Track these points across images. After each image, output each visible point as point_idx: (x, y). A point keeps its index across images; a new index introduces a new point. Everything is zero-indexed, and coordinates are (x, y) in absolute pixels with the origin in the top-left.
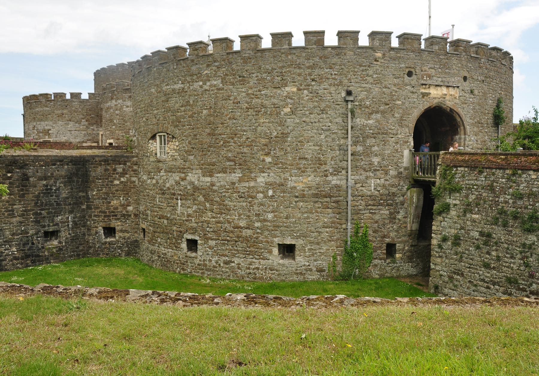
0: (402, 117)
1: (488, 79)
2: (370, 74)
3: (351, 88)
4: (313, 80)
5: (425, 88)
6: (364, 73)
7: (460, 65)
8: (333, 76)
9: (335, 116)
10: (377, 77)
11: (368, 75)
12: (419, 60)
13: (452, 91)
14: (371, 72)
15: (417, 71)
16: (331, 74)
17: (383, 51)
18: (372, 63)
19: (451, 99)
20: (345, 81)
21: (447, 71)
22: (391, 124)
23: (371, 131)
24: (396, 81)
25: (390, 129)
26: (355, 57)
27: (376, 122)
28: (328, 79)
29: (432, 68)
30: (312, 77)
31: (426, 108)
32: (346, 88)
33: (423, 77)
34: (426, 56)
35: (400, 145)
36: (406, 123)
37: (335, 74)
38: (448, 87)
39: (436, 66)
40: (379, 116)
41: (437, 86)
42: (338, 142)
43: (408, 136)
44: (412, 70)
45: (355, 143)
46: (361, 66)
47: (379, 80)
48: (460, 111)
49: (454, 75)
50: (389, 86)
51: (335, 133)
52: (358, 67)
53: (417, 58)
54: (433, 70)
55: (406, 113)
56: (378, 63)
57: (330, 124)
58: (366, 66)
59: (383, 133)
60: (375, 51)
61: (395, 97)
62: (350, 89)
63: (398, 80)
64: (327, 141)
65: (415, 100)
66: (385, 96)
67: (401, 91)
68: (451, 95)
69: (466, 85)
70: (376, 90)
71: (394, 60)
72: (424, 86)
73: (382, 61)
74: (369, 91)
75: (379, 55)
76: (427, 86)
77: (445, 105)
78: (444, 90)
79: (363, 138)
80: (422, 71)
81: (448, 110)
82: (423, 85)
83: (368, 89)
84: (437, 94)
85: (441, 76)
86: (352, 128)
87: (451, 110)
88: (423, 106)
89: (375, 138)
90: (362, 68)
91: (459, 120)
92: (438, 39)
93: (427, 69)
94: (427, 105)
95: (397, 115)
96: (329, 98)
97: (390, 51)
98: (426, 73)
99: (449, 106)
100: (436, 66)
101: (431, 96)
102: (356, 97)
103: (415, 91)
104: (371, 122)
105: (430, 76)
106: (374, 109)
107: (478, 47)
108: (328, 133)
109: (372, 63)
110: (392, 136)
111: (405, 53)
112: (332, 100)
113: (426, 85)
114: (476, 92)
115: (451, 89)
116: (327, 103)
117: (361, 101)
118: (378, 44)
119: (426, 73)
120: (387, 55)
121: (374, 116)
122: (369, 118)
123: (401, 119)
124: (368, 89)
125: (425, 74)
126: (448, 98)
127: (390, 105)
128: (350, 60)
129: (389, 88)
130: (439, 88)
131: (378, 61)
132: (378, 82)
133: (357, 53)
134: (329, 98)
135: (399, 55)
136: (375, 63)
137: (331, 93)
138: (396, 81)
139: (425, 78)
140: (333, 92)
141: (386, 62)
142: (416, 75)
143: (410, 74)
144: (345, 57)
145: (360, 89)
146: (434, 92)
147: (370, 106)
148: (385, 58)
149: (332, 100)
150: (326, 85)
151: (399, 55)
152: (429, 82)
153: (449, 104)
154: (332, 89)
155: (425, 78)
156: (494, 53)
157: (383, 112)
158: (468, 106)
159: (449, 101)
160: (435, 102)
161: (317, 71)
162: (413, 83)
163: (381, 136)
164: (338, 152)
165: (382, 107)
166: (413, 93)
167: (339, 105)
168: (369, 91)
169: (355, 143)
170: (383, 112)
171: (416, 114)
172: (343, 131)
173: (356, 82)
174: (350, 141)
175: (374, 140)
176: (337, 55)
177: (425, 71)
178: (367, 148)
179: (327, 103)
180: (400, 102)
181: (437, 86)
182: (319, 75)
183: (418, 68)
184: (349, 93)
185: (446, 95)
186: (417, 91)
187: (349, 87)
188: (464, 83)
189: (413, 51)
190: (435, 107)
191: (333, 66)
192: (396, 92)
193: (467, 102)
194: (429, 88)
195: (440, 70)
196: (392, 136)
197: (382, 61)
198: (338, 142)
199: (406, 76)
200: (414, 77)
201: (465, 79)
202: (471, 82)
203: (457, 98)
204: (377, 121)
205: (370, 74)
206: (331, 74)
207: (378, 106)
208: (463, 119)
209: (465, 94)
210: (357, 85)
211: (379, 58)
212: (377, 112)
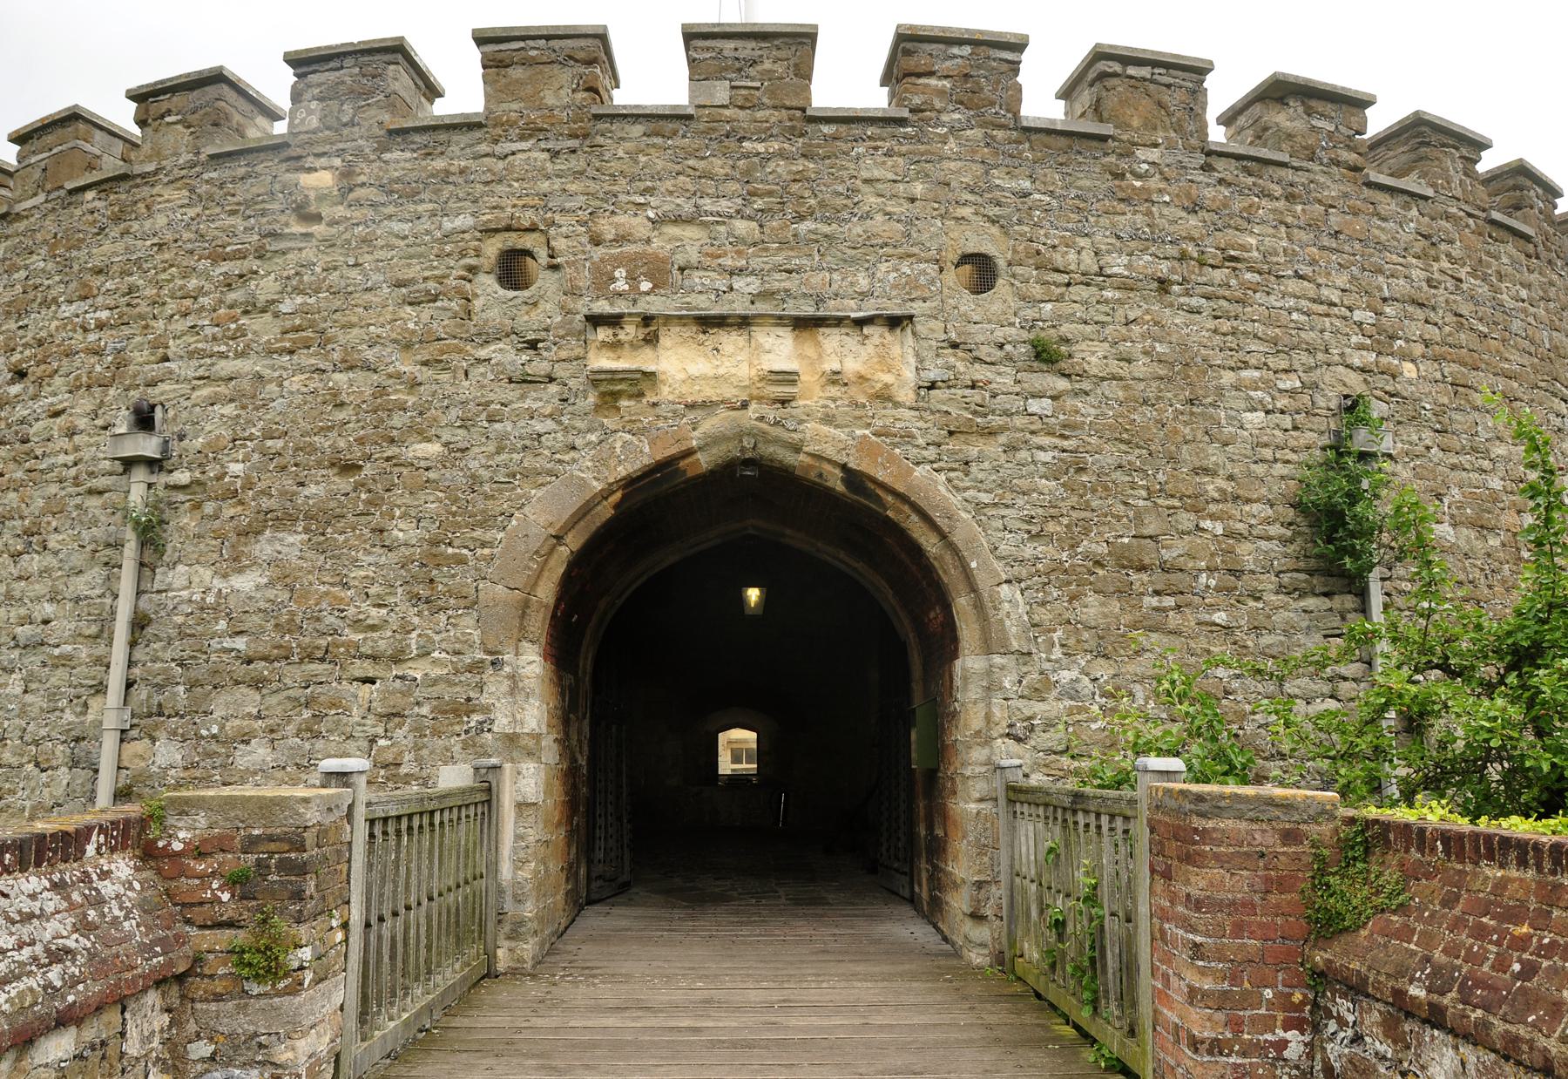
0: (435, 543)
1: (1218, 275)
2: (262, 299)
3: (163, 387)
4: (21, 375)
5: (615, 346)
6: (232, 296)
7: (918, 188)
8: (92, 337)
9: (78, 560)
10: (303, 311)
11: (251, 308)
12: (579, 174)
13: (842, 353)
14: (266, 287)
15: (560, 244)
16: (85, 330)
17: (340, 153)
18: (273, 235)
19: (842, 409)
20: (139, 356)
21: (805, 227)
22: (364, 587)
23: (240, 643)
25: (357, 624)
26: (191, 212)
27: (271, 584)
28: (69, 354)
29: (678, 220)
30: (17, 357)
31: (622, 471)
32: (135, 394)
33: (602, 280)
34: (633, 156)
35: (419, 731)
36: (463, 579)
37: (101, 326)
38: (805, 325)
39: (707, 204)
40: (292, 542)
41: (709, 323)
42: (69, 716)
43: (476, 667)
44: (528, 242)
45: (145, 722)
46: (218, 257)
47: (312, 325)
48: (929, 482)
49: (870, 249)
50: (370, 355)
51: (66, 661)
52: (204, 264)
53: (560, 165)
54: (690, 232)
55: (471, 510)
56: (315, 228)
57: (49, 609)
58: (240, 256)
60: (296, 163)
61: (398, 420)
62: (154, 394)
63: (426, 312)
64: (23, 713)
66: (341, 415)
67: (445, 377)
68: (835, 378)
69: (997, 315)
70: (293, 384)
71: (413, 196)
72: (603, 334)
73: (340, 211)
74: (249, 396)
75: (321, 180)
76: (630, 332)
77: (797, 449)
78: (779, 350)
79: (192, 685)
80: (596, 241)
81: (836, 482)
82: (595, 321)
83: (245, 384)
85: (756, 263)
86: (140, 624)
87: (854, 478)
88: (601, 462)
89: (257, 684)
90: (225, 267)
91: (930, 544)
92: (731, 44)
93: (637, 224)
94: (632, 453)
95: (402, 531)
96: (62, 458)
97: (384, 149)
98: (630, 248)
99: (830, 452)
100: (707, 204)
101: (665, 393)
102: (181, 437)
103: (540, 367)
104: (245, 583)
105: (659, 272)
106: (266, 503)
107: (1103, 76)
108: (33, 661)
109: (273, 235)
110: (369, 669)
111: (484, 148)
112: (73, 472)
113: (614, 321)
114: (1092, 356)
115: (831, 340)
116: (53, 489)
117: (201, 460)
118: (314, 122)
119: (630, 248)
120: (366, 172)
121: (264, 547)
122: (237, 564)
123: (433, 555)
124: (245, 384)
125: (618, 261)
126: (812, 396)
127: (368, 470)
128: (169, 237)
129: (369, 368)
130: (731, 341)
131: (317, 218)
132: (304, 336)
133: (203, 189)
134: (62, 458)
135: (439, 164)
136: (297, 229)
137: (71, 433)
139: (621, 285)
140: (82, 423)
141: (357, 214)
142: (555, 268)
143: (512, 270)
144: (147, 224)
145: (205, 392)
146: (680, 365)
147: (248, 484)
148: (360, 193)
149: (73, 472)
150: (57, 393)
151: (439, 164)
152: (656, 305)
153: (824, 439)
154: (85, 404)
155: (621, 285)
156: (1286, 119)
157: (320, 520)
158: (1011, 448)
159: (828, 419)
160: (706, 441)
161: (40, 322)
162: (530, 322)
163: (293, 674)
164: (63, 775)
165: (312, 489)
167: (101, 493)
168: (249, 396)
169: (145, 722)
170: (320, 520)
172: (101, 650)
173: (190, 355)
174: (109, 711)
175: (250, 700)
176: (117, 219)
177: (621, 239)
178: (209, 755)
179: (53, 489)
180: (434, 449)
181: (709, 323)
182: (40, 343)
184: (144, 420)
185: (788, 378)
186: (560, 371)
187: (152, 384)
188: (967, 303)
189: (532, 132)
190: (726, 472)
191: (96, 281)
192: (414, 384)
193: (996, 421)
194: (651, 340)
195: (741, 226)
196: (369, 669)
197: (340, 211)
198: (69, 716)
199: (488, 284)
200: (545, 283)
201: (982, 271)
202: (1037, 291)
203: (906, 395)
204: (284, 578)
205: (262, 299)
206: (85, 330)
207: (289, 483)
208: (957, 538)
209: (980, 373)
210: (188, 369)
211: (321, 198)
212: (283, 520)
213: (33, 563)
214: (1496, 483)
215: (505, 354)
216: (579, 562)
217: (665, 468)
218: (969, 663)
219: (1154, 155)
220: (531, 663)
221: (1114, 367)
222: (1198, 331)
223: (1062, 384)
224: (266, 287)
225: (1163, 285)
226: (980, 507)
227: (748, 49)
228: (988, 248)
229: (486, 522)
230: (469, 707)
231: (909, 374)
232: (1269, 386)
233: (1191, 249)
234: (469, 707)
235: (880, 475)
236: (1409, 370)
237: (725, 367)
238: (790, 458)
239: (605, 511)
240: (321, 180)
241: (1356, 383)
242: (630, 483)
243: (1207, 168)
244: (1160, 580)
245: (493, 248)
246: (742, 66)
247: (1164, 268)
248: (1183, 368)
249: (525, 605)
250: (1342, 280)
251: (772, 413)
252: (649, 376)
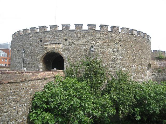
11: (28, 43)
13: (57, 46)
14: (29, 42)
24: (36, 44)
38: (55, 44)
44: (41, 39)
46: (27, 40)
59: (31, 63)
65: (42, 50)
71: (36, 36)
73: (32, 37)
75: (31, 36)
78: (54, 46)
84: (50, 47)
87: (58, 53)
93: (47, 38)
94: (46, 52)
104: (28, 59)
105: (48, 41)
113: (45, 44)
115: (57, 45)
121: (29, 57)
130: (51, 45)
132: (31, 45)
135: (37, 35)
138: (36, 44)
143: (41, 41)
146: (49, 47)
152: (48, 43)
153: (56, 51)
159: (56, 49)
161: (19, 43)
170: (31, 56)
171: (41, 55)
183: (43, 38)
192: (36, 48)
195: (52, 38)
197: (32, 37)
212: (30, 56)
213: (19, 58)
214: (106, 51)
215: (40, 46)
216: (44, 58)
217: (48, 53)
219: (78, 31)
220: (41, 64)
221: (74, 45)
222: (80, 42)
223: (71, 46)
224: (29, 42)
225: (78, 40)
226: (65, 54)
227: (53, 27)
228: (67, 38)
229: (39, 56)
231: (61, 46)
232: (85, 46)
233: (80, 37)
235: (59, 53)
236: (98, 43)
237: (51, 46)
238: (55, 52)
239: (45, 55)
240: (31, 36)
242: (46, 53)
243: (82, 31)
244: (76, 58)
245: (39, 40)
246: (53, 28)
247: (78, 38)
250: (92, 38)
251: (53, 49)
252: (47, 48)
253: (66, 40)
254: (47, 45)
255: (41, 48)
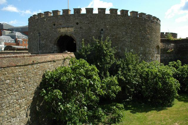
13: (69, 29)
31: (59, 36)
78: (66, 29)
84: (63, 31)
94: (60, 35)
95: (50, 39)
104: (44, 42)
105: (61, 25)
114: (84, 28)
122: (43, 41)
132: (45, 29)
143: (54, 25)
153: (69, 34)
166: (55, 31)
168: (43, 32)
201: (77, 24)
214: (115, 34)
218: (77, 46)
223: (82, 30)
224: (44, 26)
225: (89, 23)
230: (53, 49)
234: (53, 49)
235: (72, 36)
236: (108, 27)
239: (59, 38)
240: (45, 20)
241: (102, 28)
248: (90, 28)
249: (55, 43)
253: (77, 24)
254: (60, 29)
255: (55, 31)
